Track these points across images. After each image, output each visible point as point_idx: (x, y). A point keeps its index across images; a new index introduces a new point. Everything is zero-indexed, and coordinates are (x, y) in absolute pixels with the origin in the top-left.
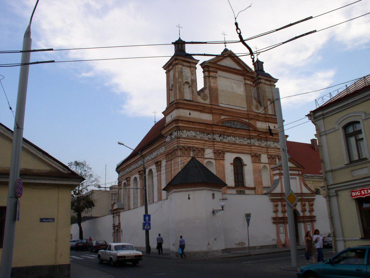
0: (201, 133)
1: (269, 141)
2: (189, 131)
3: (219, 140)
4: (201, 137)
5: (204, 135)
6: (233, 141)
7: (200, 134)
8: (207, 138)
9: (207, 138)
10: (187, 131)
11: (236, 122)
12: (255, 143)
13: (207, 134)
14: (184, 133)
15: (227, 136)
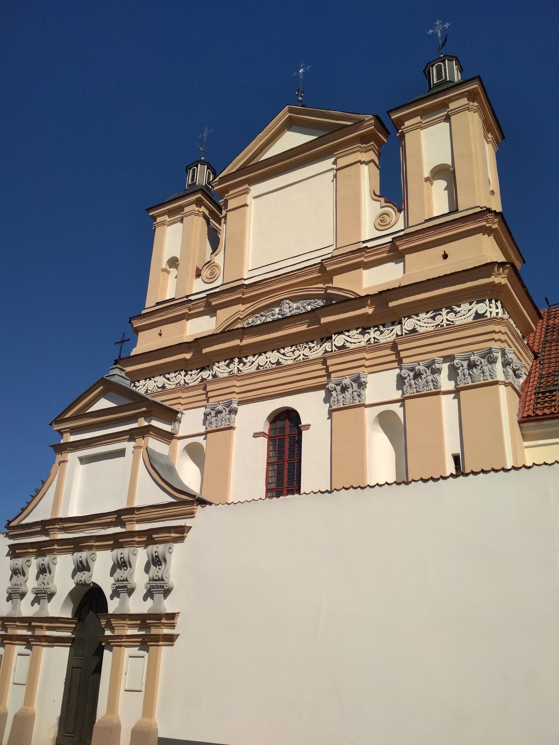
0: (180, 374)
1: (410, 317)
2: (150, 379)
3: (226, 375)
4: (177, 384)
5: (191, 375)
6: (273, 364)
7: (175, 377)
8: (196, 380)
9: (196, 380)
10: (146, 380)
11: (288, 301)
12: (348, 345)
13: (199, 371)
14: (140, 387)
15: (254, 355)
